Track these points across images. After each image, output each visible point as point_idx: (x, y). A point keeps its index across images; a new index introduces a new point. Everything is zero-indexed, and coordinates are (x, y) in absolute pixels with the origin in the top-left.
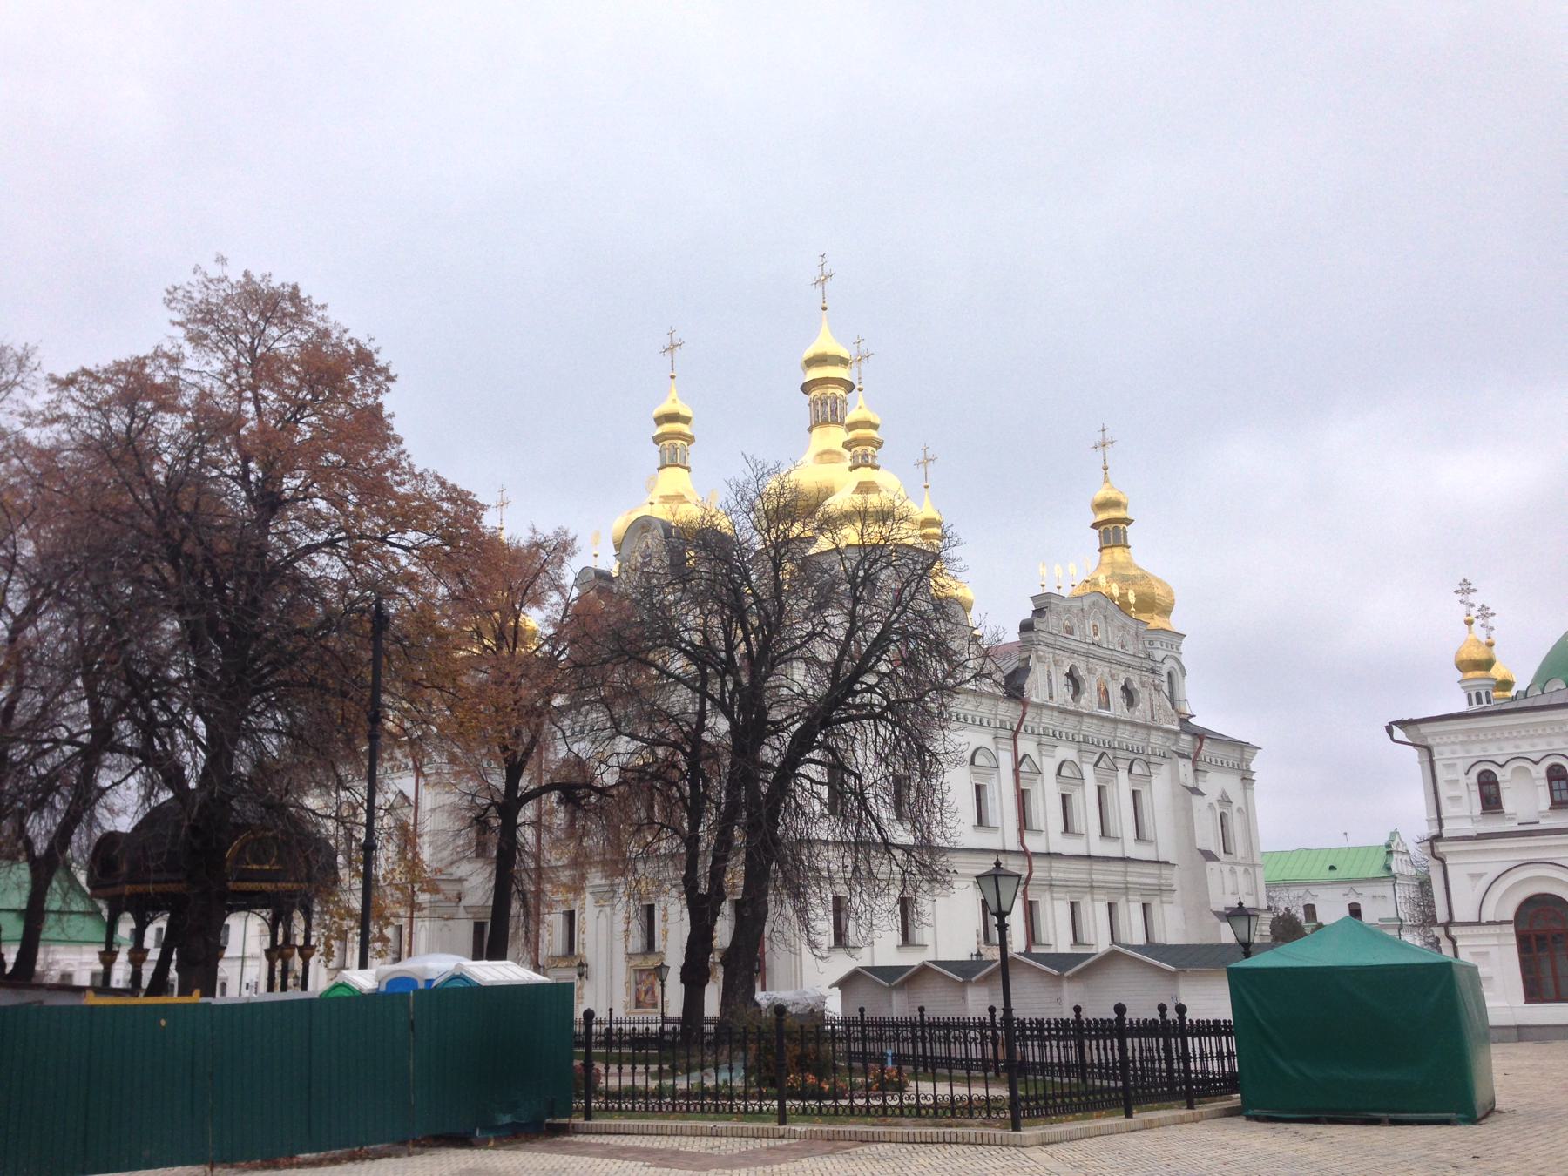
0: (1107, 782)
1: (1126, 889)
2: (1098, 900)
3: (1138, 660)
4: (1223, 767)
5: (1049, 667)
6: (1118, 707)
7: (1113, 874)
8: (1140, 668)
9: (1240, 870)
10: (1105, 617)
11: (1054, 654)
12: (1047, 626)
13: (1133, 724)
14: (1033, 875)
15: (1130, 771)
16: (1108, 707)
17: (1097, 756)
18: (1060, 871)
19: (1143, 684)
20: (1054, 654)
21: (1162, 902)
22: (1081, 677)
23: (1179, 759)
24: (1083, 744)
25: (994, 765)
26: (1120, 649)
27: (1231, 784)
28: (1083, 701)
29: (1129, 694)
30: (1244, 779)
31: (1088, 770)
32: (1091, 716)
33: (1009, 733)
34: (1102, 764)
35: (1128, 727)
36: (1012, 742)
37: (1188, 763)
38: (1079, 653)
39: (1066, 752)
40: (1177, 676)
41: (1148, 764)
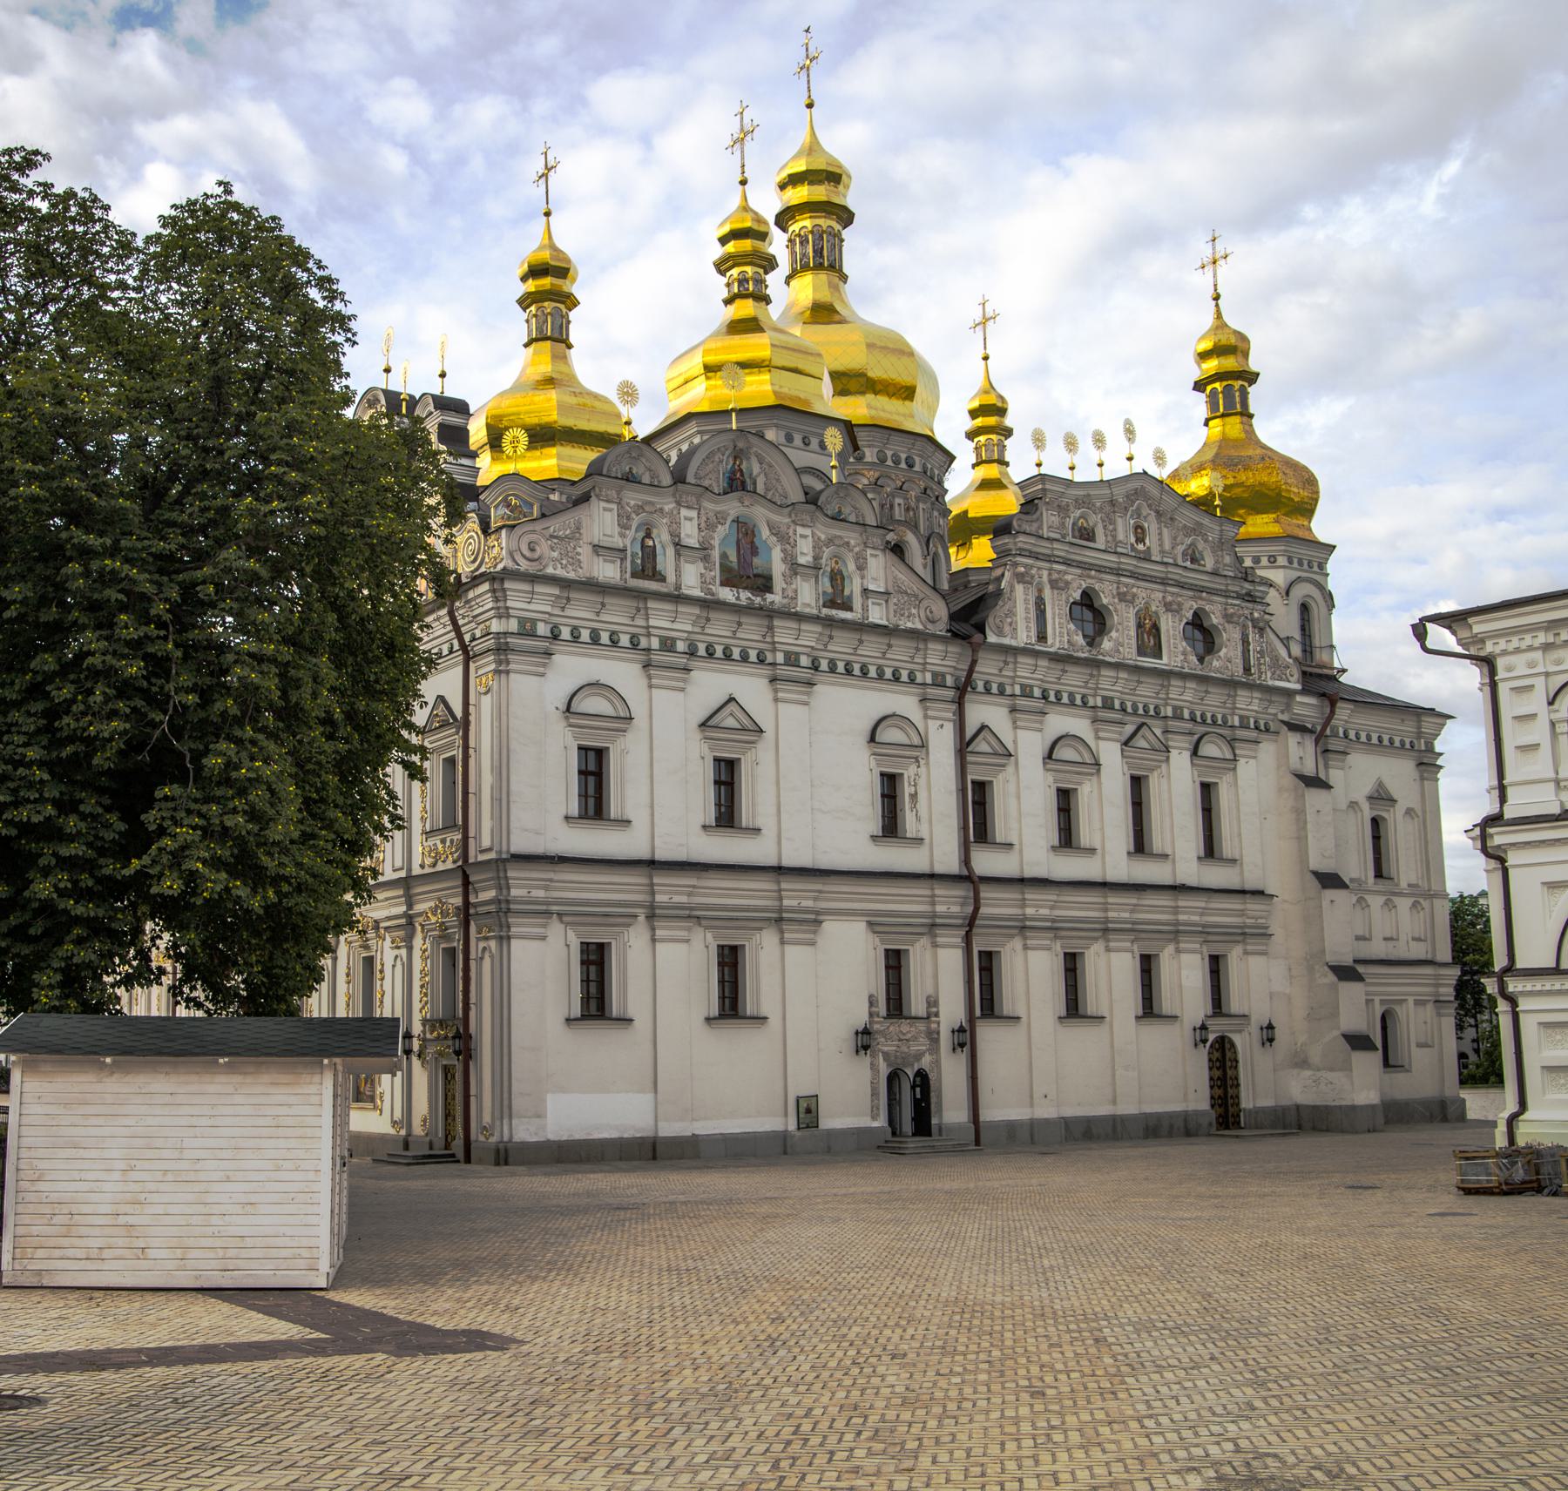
0: (1152, 770)
1: (1175, 934)
2: (663, 940)
4: (1383, 746)
5: (1040, 591)
6: (1176, 651)
7: (1156, 910)
8: (1225, 594)
9: (1404, 904)
10: (1157, 512)
11: (1118, 583)
12: (1040, 527)
13: (1203, 679)
14: (983, 910)
15: (1195, 753)
16: (1157, 652)
17: (1130, 729)
18: (1038, 906)
19: (1228, 618)
20: (1050, 570)
22: (1105, 607)
23: (1290, 734)
24: (1104, 712)
25: (916, 741)
26: (1188, 564)
27: (1397, 773)
28: (1107, 645)
29: (1202, 633)
30: (1421, 764)
31: (1110, 754)
32: (1117, 666)
33: (951, 694)
34: (1142, 743)
35: (1191, 685)
36: (954, 707)
37: (1309, 743)
38: (1211, 592)
39: (1060, 722)
40: (1317, 610)
41: (1231, 742)
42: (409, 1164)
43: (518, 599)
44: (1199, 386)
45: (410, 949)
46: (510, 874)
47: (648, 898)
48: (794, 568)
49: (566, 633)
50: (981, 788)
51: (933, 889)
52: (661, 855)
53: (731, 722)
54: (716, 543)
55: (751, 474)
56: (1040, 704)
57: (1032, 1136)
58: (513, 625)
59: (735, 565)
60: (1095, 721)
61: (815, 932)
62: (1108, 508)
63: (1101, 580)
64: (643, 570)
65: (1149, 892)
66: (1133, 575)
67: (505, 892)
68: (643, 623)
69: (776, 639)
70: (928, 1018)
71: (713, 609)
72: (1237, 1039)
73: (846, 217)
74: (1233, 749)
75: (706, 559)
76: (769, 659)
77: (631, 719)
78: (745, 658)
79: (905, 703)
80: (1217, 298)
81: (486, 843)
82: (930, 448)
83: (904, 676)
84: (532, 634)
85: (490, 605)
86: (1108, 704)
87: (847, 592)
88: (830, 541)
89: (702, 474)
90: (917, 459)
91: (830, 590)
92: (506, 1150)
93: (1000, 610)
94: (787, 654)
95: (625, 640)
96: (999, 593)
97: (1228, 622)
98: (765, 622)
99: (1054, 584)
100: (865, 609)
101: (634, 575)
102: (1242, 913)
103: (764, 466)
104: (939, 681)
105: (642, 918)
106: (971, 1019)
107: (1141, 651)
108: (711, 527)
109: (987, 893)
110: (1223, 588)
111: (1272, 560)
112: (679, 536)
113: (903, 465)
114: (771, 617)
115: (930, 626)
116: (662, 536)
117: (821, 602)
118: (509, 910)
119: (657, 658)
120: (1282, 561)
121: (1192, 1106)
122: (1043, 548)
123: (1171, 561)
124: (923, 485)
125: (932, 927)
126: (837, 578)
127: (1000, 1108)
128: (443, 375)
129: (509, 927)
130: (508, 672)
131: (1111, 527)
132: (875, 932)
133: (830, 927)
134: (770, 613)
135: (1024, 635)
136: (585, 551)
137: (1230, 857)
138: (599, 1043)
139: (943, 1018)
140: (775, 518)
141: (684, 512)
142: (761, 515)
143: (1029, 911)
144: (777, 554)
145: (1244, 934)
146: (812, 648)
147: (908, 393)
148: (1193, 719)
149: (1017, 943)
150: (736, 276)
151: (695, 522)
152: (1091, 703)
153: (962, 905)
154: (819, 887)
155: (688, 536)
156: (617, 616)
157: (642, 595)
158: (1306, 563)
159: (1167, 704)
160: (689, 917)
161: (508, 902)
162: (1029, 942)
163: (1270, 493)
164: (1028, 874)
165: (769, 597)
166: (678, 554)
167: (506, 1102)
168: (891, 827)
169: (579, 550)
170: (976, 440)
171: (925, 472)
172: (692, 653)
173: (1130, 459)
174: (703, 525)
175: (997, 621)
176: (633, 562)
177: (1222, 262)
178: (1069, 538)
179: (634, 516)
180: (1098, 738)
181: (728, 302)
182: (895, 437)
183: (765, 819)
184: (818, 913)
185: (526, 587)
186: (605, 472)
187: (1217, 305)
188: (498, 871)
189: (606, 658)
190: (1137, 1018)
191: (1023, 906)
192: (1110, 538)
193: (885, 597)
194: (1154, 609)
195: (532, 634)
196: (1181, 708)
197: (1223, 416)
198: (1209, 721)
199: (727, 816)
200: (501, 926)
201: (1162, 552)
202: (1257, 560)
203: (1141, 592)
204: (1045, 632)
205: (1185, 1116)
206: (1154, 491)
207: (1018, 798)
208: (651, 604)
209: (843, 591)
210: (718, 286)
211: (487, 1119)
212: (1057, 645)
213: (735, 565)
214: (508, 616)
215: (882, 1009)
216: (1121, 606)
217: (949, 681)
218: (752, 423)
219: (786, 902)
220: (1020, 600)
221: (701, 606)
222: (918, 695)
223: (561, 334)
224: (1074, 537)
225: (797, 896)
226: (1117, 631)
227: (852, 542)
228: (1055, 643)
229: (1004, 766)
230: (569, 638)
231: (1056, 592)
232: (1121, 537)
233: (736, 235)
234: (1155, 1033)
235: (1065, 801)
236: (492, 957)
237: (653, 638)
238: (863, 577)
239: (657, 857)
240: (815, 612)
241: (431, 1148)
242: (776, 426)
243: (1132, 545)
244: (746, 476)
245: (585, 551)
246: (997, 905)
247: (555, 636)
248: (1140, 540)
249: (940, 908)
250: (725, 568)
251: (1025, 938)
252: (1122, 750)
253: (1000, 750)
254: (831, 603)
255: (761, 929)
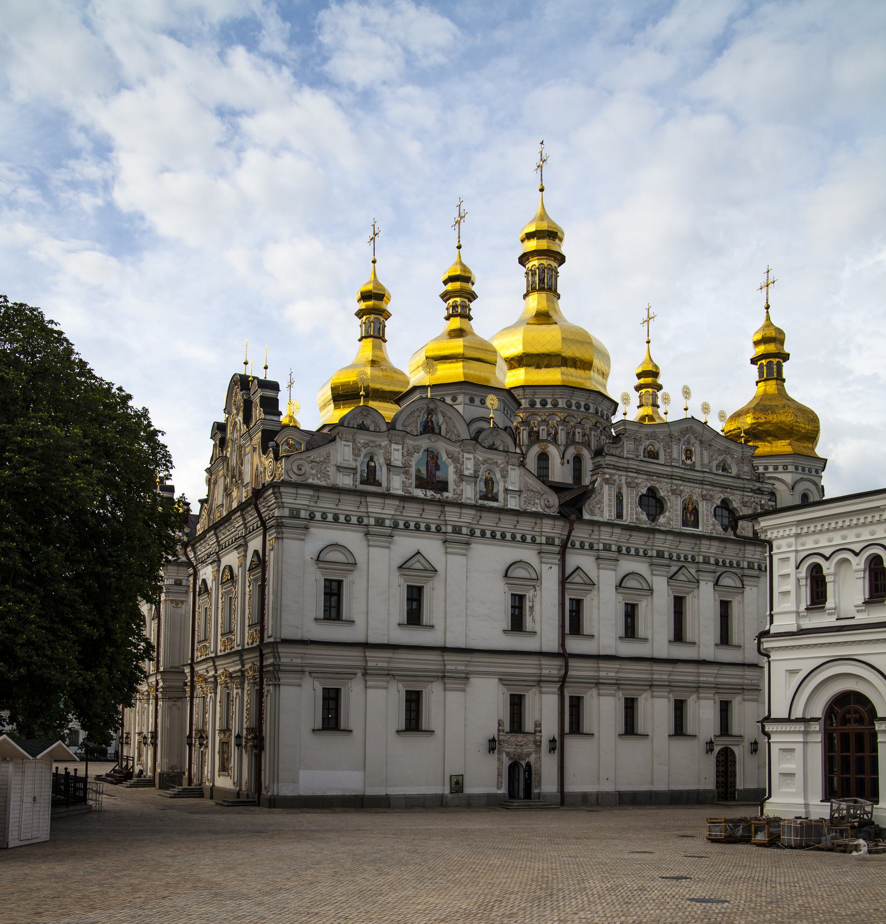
0: (688, 593)
1: (697, 688)
3: (741, 481)
5: (620, 488)
6: (708, 523)
7: (685, 674)
8: (743, 489)
10: (701, 441)
12: (623, 451)
14: (570, 673)
15: (716, 584)
17: (674, 569)
18: (608, 671)
21: (699, 698)
24: (658, 559)
25: (534, 576)
26: (720, 472)
28: (662, 520)
31: (660, 584)
32: (666, 533)
34: (681, 577)
35: (715, 543)
39: (627, 565)
42: (228, 806)
43: (289, 497)
44: (754, 361)
45: (243, 689)
46: (279, 650)
47: (364, 664)
48: (461, 477)
49: (318, 516)
50: (577, 604)
51: (540, 661)
52: (372, 640)
53: (418, 566)
54: (413, 463)
55: (438, 423)
56: (615, 555)
57: (597, 800)
58: (286, 512)
59: (425, 476)
60: (651, 564)
61: (465, 684)
62: (667, 439)
63: (660, 482)
64: (368, 480)
65: (679, 664)
66: (682, 479)
67: (278, 660)
68: (364, 510)
69: (447, 518)
70: (535, 733)
71: (407, 501)
72: (736, 749)
73: (561, 259)
74: (742, 581)
75: (406, 473)
76: (443, 529)
77: (356, 564)
78: (428, 529)
79: (529, 554)
80: (767, 308)
81: (270, 633)
82: (600, 399)
83: (529, 539)
84: (297, 517)
85: (273, 501)
86: (660, 555)
87: (495, 491)
88: (485, 462)
89: (407, 424)
90: (591, 406)
91: (484, 490)
92: (274, 800)
93: (593, 500)
94: (454, 527)
95: (354, 520)
96: (593, 490)
97: (744, 506)
98: (440, 509)
99: (629, 485)
100: (506, 500)
101: (362, 483)
102: (742, 677)
103: (446, 418)
104: (550, 541)
105: (359, 675)
106: (562, 734)
107: (685, 523)
108: (410, 454)
109: (572, 663)
110: (742, 486)
111: (785, 467)
112: (390, 460)
113: (582, 409)
114: (444, 506)
115: (547, 510)
116: (380, 460)
117: (478, 496)
118: (280, 670)
119: (373, 530)
120: (791, 468)
121: (702, 787)
122: (623, 463)
123: (708, 470)
124: (594, 421)
125: (539, 682)
126: (489, 482)
127: (574, 786)
128: (266, 368)
129: (279, 679)
130: (282, 538)
131: (669, 451)
132: (504, 685)
133: (475, 681)
134: (443, 503)
135: (607, 514)
136: (332, 470)
137: (691, 641)
138: (332, 742)
139: (544, 733)
140: (451, 448)
141: (394, 446)
142: (442, 447)
143: (602, 674)
144: (451, 469)
145: (743, 689)
146: (470, 523)
147: (586, 365)
148: (717, 563)
149: (594, 692)
150: (451, 304)
151: (401, 452)
152: (650, 554)
153: (559, 670)
154: (304, 651)
155: (396, 460)
156: (348, 505)
157: (364, 494)
158: (807, 469)
159: (699, 555)
160: (388, 674)
161: (279, 665)
162: (601, 691)
163: (786, 428)
164: (602, 653)
165: (445, 494)
166: (389, 470)
167: (276, 774)
168: (517, 624)
169: (328, 469)
170: (640, 392)
171: (597, 413)
172: (395, 526)
173: (686, 409)
174: (405, 453)
175: (591, 506)
176: (361, 475)
177: (771, 286)
178: (641, 457)
179: (363, 449)
180: (653, 575)
181: (447, 318)
182: (576, 393)
183: (438, 621)
184: (467, 674)
185: (293, 490)
186: (346, 424)
187: (767, 312)
188: (274, 648)
189: (342, 530)
190: (670, 736)
191: (599, 671)
192: (667, 457)
193: (519, 493)
194: (695, 498)
195: (297, 517)
196: (709, 557)
197: (766, 380)
198: (728, 564)
199: (414, 617)
200: (275, 678)
201: (702, 465)
202: (766, 468)
203: (687, 489)
204: (622, 513)
205: (698, 792)
206: (699, 429)
207: (599, 609)
208: (369, 499)
209: (492, 490)
210: (442, 308)
211: (267, 783)
212: (629, 521)
213: (425, 476)
214: (284, 507)
215: (507, 727)
216: (673, 498)
217: (557, 541)
218: (439, 392)
219: (448, 667)
220: (607, 495)
221: (400, 500)
222: (537, 550)
223: (379, 333)
224: (644, 457)
225: (454, 663)
226: (670, 512)
227: (499, 462)
228: (627, 519)
229: (590, 591)
230: (321, 519)
231: (629, 489)
232: (675, 455)
233: (451, 279)
234: (681, 746)
235: (631, 612)
236: (271, 695)
237: (371, 519)
238: (505, 482)
239: (369, 641)
240: (473, 502)
241: (248, 798)
242: (464, 393)
243: (683, 461)
244: (435, 425)
245: (332, 470)
246: (578, 669)
247: (312, 517)
248: (689, 457)
249: (544, 672)
250: (418, 478)
251: (599, 689)
252: (668, 582)
253: (588, 581)
254: (484, 497)
255: (432, 682)
